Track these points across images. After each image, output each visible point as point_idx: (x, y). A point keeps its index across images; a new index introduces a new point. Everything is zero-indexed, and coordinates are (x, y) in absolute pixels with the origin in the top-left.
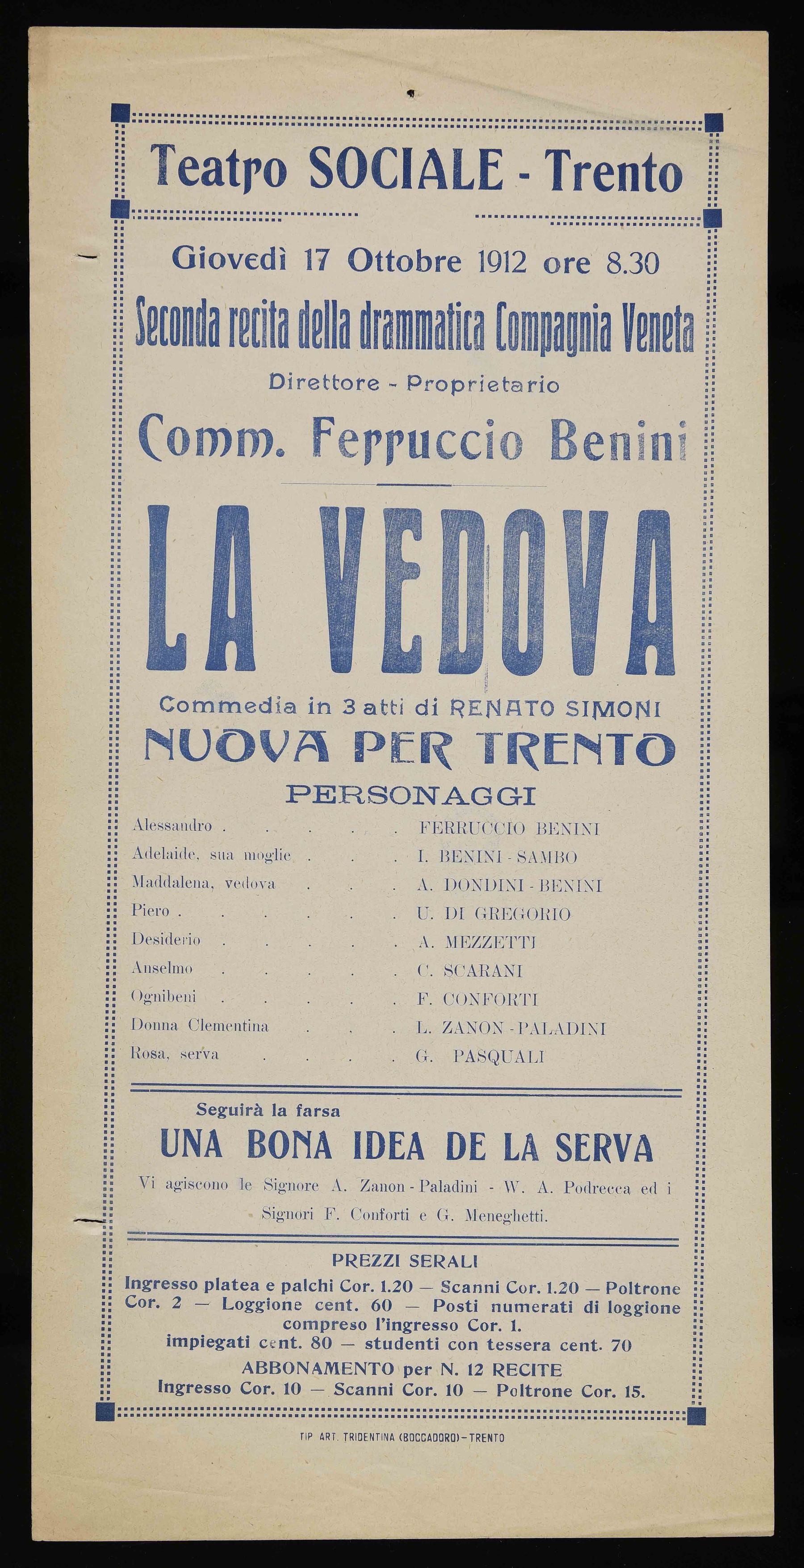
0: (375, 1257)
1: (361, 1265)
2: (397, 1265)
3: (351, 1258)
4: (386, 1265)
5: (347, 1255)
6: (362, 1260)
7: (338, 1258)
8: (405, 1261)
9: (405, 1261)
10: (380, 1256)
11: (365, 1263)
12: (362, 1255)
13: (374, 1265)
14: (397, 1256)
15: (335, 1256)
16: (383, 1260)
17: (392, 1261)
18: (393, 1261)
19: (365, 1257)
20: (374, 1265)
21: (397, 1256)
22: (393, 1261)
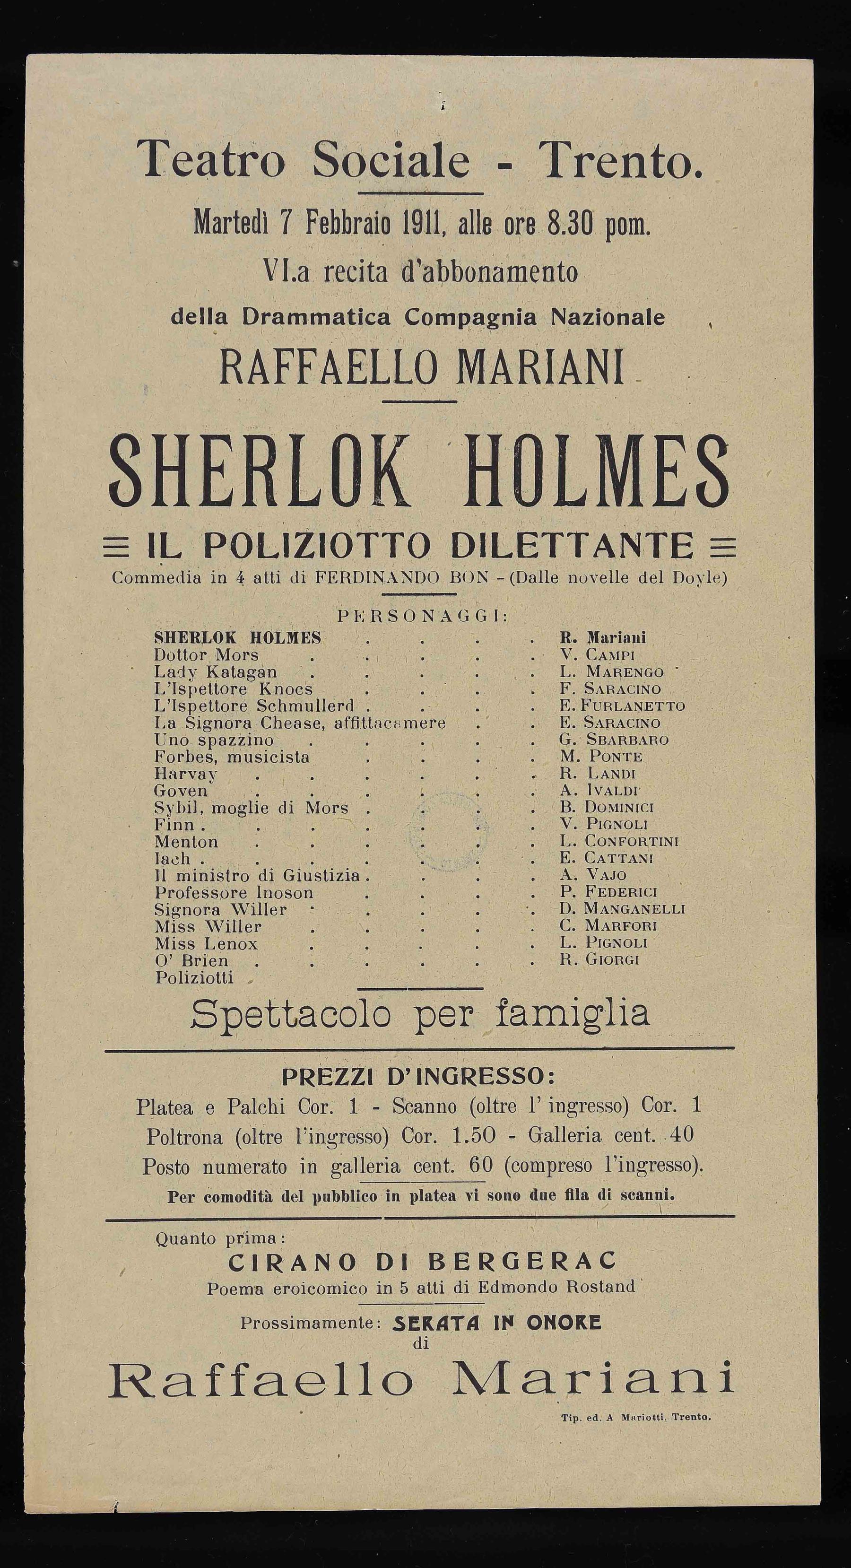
0: (340, 1072)
1: (320, 1083)
2: (370, 1083)
3: (307, 1074)
4: (354, 1083)
5: (302, 1071)
6: (321, 1076)
7: (290, 1074)
8: (381, 1077)
9: (381, 1077)
10: (345, 1070)
11: (325, 1080)
12: (320, 1070)
13: (338, 1083)
14: (370, 1071)
15: (285, 1071)
16: (350, 1076)
17: (363, 1076)
18: (364, 1077)
19: (325, 1072)
20: (338, 1083)
21: (370, 1071)
22: (364, 1077)
